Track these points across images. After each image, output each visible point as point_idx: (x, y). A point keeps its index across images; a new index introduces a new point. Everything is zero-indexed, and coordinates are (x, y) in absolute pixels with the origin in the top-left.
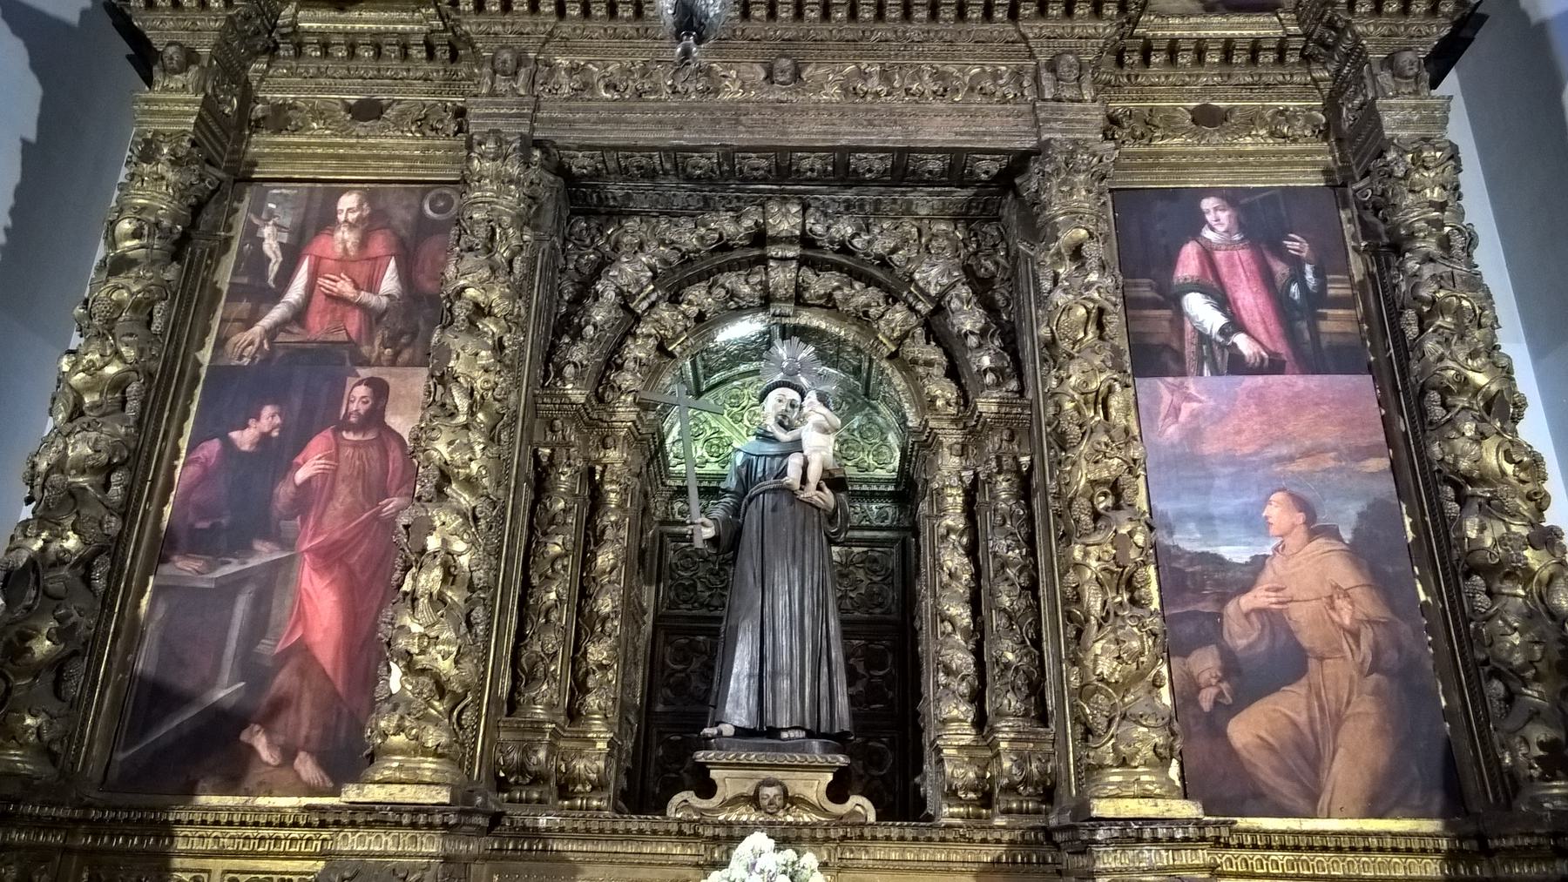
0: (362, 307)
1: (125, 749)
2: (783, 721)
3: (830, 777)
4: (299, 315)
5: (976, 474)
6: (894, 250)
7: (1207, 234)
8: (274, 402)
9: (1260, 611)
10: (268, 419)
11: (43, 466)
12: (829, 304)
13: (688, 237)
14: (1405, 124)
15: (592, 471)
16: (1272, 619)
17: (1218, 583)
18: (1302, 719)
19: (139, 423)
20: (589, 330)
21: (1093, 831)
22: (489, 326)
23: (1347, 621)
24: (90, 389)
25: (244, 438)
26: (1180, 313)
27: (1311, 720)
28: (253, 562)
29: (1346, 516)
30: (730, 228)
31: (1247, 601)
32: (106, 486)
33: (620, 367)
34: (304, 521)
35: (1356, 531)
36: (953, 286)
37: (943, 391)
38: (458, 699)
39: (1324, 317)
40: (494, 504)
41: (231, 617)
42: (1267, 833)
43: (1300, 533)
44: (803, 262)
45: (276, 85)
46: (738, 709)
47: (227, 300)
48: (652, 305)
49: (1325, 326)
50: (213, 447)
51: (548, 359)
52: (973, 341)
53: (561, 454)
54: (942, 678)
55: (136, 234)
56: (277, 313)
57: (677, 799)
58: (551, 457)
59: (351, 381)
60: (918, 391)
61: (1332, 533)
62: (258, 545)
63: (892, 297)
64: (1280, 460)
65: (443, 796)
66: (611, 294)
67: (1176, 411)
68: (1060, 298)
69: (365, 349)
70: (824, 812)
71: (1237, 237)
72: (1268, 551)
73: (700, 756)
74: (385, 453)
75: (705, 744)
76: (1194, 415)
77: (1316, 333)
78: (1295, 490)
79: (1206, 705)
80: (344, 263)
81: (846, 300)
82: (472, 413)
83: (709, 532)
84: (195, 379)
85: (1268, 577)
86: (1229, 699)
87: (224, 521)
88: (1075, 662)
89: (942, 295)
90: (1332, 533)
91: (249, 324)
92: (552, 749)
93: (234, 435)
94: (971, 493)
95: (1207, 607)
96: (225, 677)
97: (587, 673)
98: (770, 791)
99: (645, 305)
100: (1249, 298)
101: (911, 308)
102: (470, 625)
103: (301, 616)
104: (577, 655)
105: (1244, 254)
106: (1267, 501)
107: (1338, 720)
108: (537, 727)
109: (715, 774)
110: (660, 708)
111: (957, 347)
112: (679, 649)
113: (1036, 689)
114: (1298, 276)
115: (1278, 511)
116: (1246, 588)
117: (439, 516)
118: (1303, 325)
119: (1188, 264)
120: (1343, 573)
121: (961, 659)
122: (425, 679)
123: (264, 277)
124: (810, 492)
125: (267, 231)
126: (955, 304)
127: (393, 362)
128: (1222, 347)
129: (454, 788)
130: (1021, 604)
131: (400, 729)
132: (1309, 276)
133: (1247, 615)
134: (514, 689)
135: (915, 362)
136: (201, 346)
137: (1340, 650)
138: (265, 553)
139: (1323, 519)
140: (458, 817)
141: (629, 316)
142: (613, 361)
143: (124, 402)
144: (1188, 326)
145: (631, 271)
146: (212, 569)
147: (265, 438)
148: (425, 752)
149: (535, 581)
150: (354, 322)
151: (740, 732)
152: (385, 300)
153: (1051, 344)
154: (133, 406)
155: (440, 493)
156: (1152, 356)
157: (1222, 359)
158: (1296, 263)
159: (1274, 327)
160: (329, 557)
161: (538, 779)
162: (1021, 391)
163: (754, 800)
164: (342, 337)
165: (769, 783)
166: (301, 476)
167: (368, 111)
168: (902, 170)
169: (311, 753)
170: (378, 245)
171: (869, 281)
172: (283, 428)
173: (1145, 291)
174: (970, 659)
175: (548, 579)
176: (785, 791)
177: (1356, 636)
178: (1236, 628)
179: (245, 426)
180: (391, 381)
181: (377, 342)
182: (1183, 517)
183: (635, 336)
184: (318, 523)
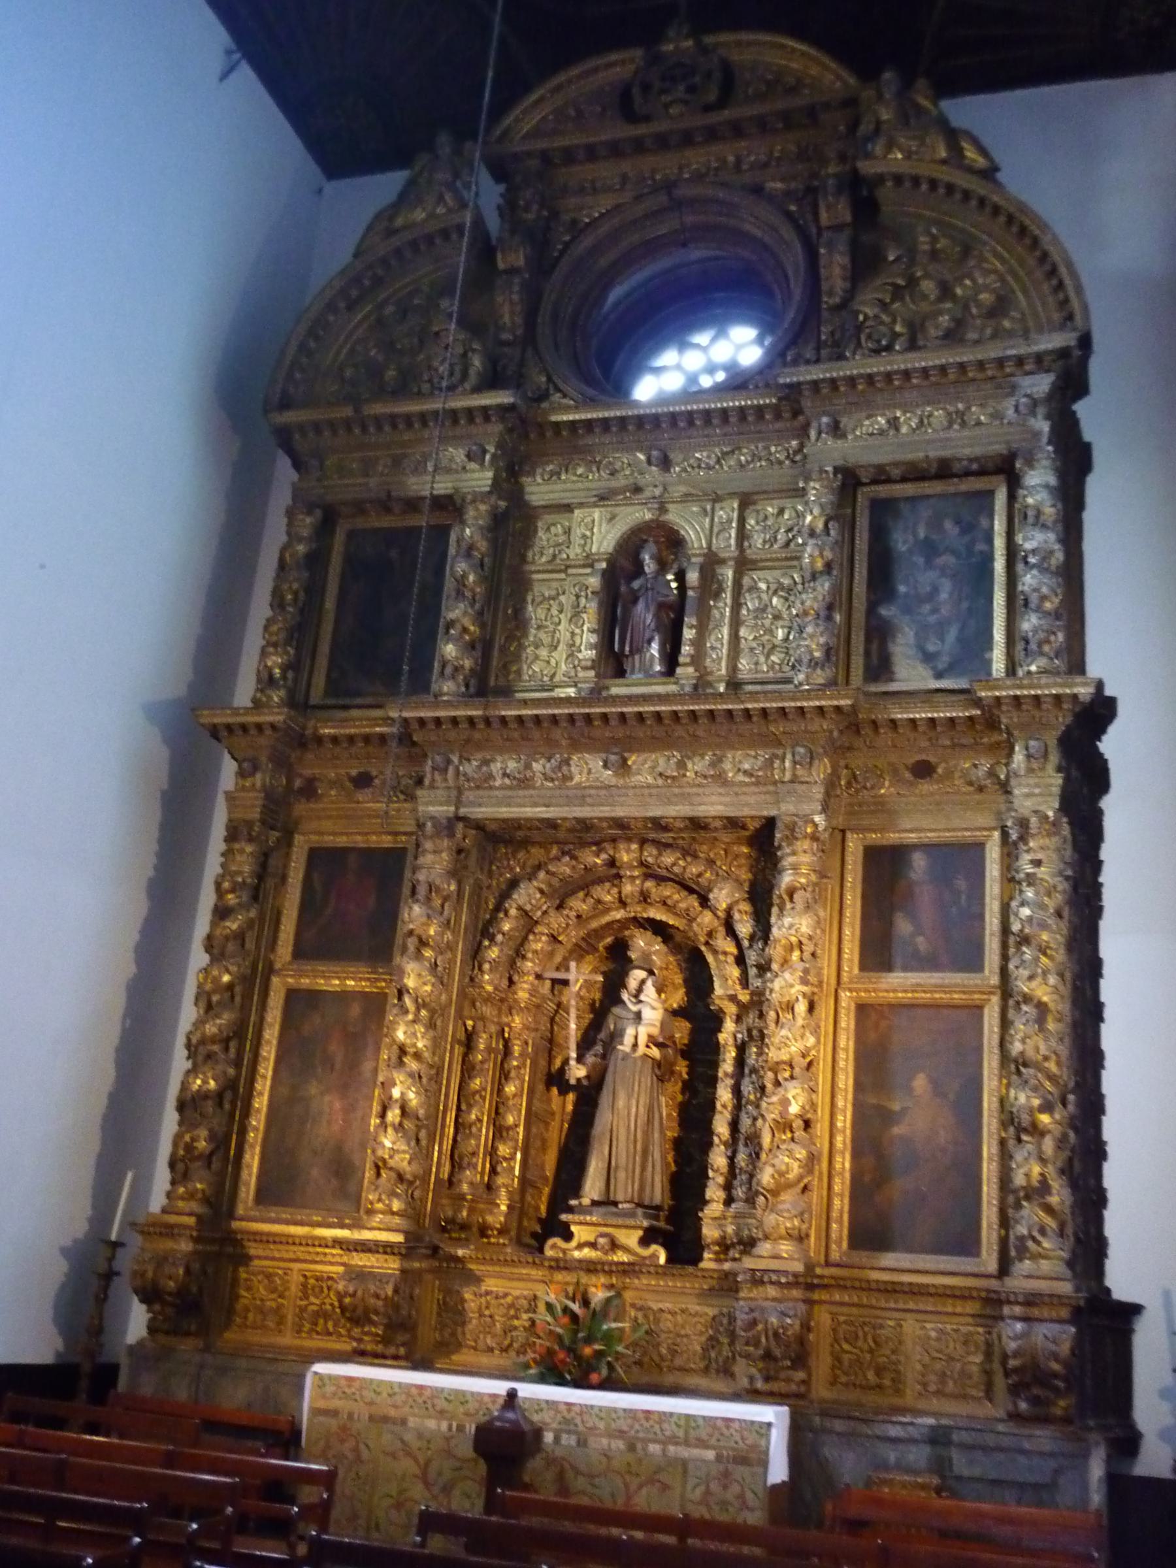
11: (194, 1041)
13: (564, 868)
14: (1028, 796)
19: (242, 1007)
20: (499, 938)
22: (428, 953)
24: (214, 991)
32: (227, 1049)
33: (524, 957)
36: (737, 902)
38: (411, 1183)
40: (431, 1067)
45: (310, 766)
51: (474, 957)
52: (746, 943)
53: (480, 1024)
57: (551, 1242)
65: (399, 1238)
70: (635, 1254)
82: (418, 1009)
92: (471, 1210)
94: (741, 1049)
102: (418, 1140)
104: (492, 1152)
108: (462, 1197)
109: (573, 1228)
117: (399, 1077)
129: (406, 1233)
131: (380, 1200)
134: (451, 1174)
140: (406, 1252)
141: (529, 923)
143: (232, 997)
145: (526, 895)
148: (393, 1213)
154: (238, 999)
155: (401, 1063)
161: (464, 1227)
167: (363, 781)
168: (697, 824)
171: (691, 891)
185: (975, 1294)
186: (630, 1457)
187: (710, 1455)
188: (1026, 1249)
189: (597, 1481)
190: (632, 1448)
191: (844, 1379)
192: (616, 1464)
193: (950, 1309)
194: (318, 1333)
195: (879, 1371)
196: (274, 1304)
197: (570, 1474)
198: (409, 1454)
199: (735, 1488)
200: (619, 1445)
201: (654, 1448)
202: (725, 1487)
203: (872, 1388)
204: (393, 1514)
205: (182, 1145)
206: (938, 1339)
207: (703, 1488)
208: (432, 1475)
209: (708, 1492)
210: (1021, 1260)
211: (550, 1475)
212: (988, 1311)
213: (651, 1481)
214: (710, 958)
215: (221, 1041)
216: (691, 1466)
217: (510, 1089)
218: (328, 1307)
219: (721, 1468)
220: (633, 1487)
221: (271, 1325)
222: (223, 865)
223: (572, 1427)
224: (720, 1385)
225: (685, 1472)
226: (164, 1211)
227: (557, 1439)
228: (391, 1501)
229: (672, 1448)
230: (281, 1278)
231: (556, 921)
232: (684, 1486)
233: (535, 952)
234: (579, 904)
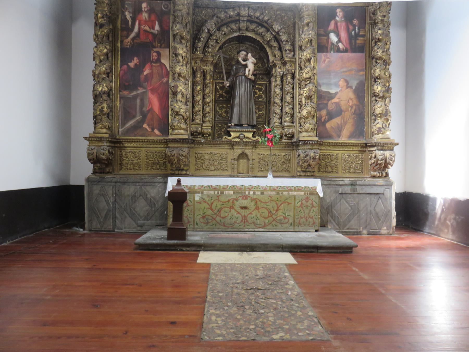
0: (152, 33)
1: (122, 128)
2: (243, 123)
3: (252, 133)
4: (138, 35)
5: (283, 73)
6: (268, 20)
7: (337, 18)
8: (137, 57)
9: (335, 103)
10: (136, 60)
11: (97, 73)
12: (254, 31)
15: (204, 71)
16: (337, 104)
17: (328, 97)
18: (340, 123)
20: (202, 39)
21: (299, 142)
23: (351, 105)
25: (132, 65)
26: (328, 38)
27: (341, 123)
28: (139, 92)
29: (354, 84)
30: (232, 13)
31: (333, 101)
32: (108, 77)
34: (148, 83)
35: (356, 87)
37: (277, 53)
39: (358, 39)
41: (137, 103)
42: (330, 143)
43: (345, 87)
44: (248, 21)
46: (235, 120)
47: (121, 31)
48: (214, 32)
49: (358, 42)
50: (125, 67)
54: (274, 115)
55: (103, 17)
56: (133, 35)
57: (224, 137)
58: (196, 69)
59: (152, 52)
60: (272, 53)
61: (351, 87)
62: (139, 88)
63: (268, 30)
64: (344, 72)
66: (206, 30)
67: (325, 61)
68: (303, 36)
69: (154, 44)
71: (343, 19)
72: (338, 91)
73: (229, 129)
74: (162, 68)
75: (229, 127)
76: (329, 62)
77: (356, 43)
78: (346, 78)
79: (323, 120)
80: (146, 22)
81: (257, 30)
83: (228, 85)
84: (118, 51)
85: (338, 96)
86: (327, 119)
87: (131, 83)
88: (299, 112)
89: (279, 31)
90: (351, 87)
91: (127, 37)
93: (129, 64)
95: (325, 102)
96: (138, 114)
97: (206, 114)
98: (242, 136)
99: (213, 32)
100: (343, 35)
101: (272, 33)
103: (150, 103)
105: (344, 24)
106: (340, 80)
107: (346, 123)
110: (217, 119)
111: (281, 43)
112: (220, 107)
113: (292, 116)
114: (354, 29)
115: (342, 83)
116: (333, 98)
118: (353, 41)
119: (332, 26)
120: (351, 95)
121: (278, 111)
122: (180, 116)
123: (128, 25)
124: (250, 77)
125: (127, 13)
126: (281, 34)
127: (161, 47)
128: (336, 46)
130: (290, 101)
132: (357, 30)
133: (333, 104)
135: (272, 46)
136: (118, 43)
137: (348, 110)
138: (141, 90)
139: (350, 85)
141: (210, 35)
142: (206, 46)
143: (108, 58)
144: (330, 41)
146: (131, 93)
147: (136, 65)
149: (195, 96)
150: (150, 37)
151: (236, 125)
152: (156, 32)
153: (301, 47)
156: (322, 47)
157: (336, 49)
158: (354, 26)
159: (348, 42)
160: (153, 91)
162: (294, 55)
163: (239, 137)
164: (148, 41)
165: (242, 134)
166: (145, 73)
169: (157, 129)
170: (153, 17)
171: (263, 26)
172: (139, 62)
173: (322, 32)
174: (280, 111)
175: (198, 95)
176: (244, 136)
177: (352, 107)
178: (330, 106)
179: (131, 62)
180: (161, 52)
181: (156, 42)
182: (323, 84)
183: (211, 39)
184: (151, 84)
185: (359, 145)
186: (278, 196)
187: (302, 193)
188: (382, 131)
189: (268, 204)
190: (278, 193)
191: (322, 170)
192: (273, 198)
193: (352, 149)
194: (154, 169)
195: (332, 167)
196: (137, 162)
197: (259, 203)
198: (205, 202)
199: (310, 202)
200: (274, 193)
201: (285, 193)
202: (307, 202)
203: (330, 172)
204: (202, 220)
205: (98, 110)
206: (348, 158)
207: (300, 203)
208: (214, 207)
209: (302, 204)
210: (378, 134)
211: (253, 204)
212: (362, 149)
213: (284, 202)
214: (268, 49)
215: (106, 73)
216: (297, 197)
217: (208, 90)
218: (156, 161)
219: (306, 197)
220: (279, 204)
221: (137, 168)
222: (96, 9)
223: (259, 189)
224: (286, 174)
225: (295, 199)
226: (94, 133)
227: (254, 193)
228: (200, 216)
229: (290, 193)
230: (138, 153)
231: (218, 34)
232: (295, 203)
233: (212, 45)
234: (225, 30)
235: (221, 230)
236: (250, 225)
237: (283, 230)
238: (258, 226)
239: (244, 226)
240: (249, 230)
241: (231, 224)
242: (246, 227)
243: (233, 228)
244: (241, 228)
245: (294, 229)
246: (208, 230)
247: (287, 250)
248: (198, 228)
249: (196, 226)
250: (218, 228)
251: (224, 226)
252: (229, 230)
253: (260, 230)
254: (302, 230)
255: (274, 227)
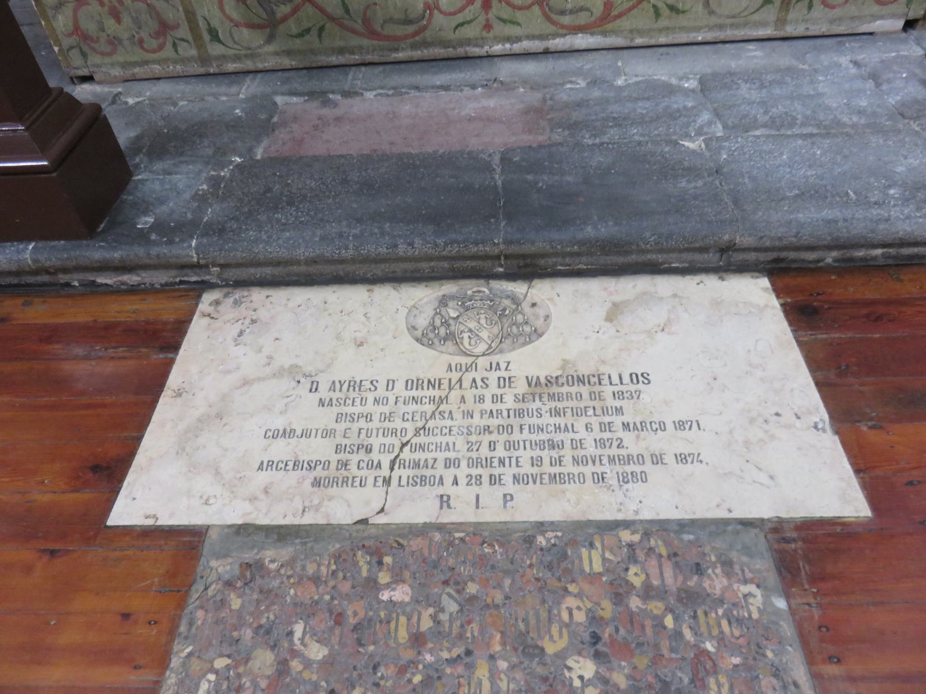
235: (357, 58)
236: (519, 16)
237: (710, 36)
238: (566, 20)
239: (488, 27)
240: (517, 47)
241: (408, 22)
242: (499, 29)
243: (425, 44)
244: (468, 42)
245: (781, 22)
246: (287, 62)
247: (752, 256)
248: (223, 58)
249: (215, 50)
250: (341, 51)
251: (373, 34)
252: (401, 55)
253: (581, 41)
254: (824, 29)
255: (663, 22)
